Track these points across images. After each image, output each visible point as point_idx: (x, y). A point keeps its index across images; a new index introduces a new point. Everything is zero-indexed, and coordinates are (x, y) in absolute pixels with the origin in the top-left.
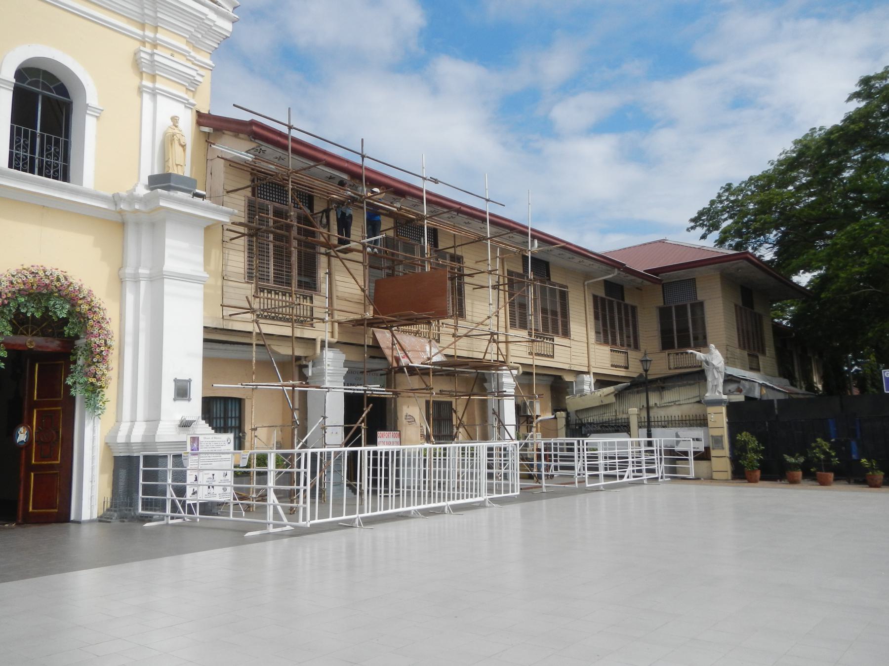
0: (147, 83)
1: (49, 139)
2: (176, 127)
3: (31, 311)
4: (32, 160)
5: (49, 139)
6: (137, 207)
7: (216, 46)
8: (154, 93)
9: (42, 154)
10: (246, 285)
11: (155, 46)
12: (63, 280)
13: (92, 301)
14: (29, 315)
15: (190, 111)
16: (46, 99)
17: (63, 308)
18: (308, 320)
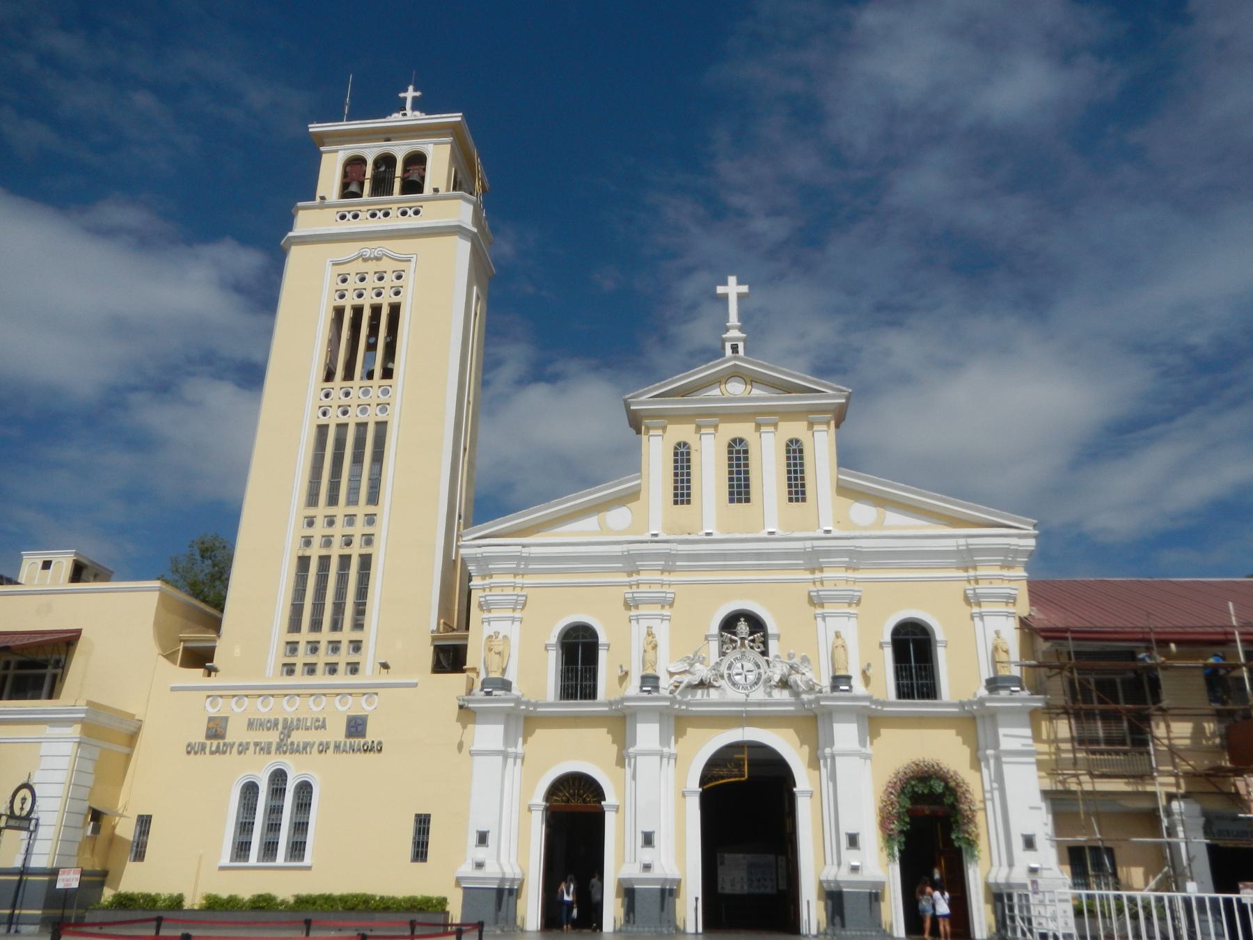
0: (976, 610)
1: (920, 668)
2: (999, 638)
3: (920, 789)
4: (912, 684)
5: (920, 668)
6: (975, 707)
7: (1026, 560)
8: (981, 616)
9: (917, 680)
11: (977, 581)
12: (936, 767)
13: (957, 778)
14: (920, 792)
15: (1012, 619)
16: (916, 643)
17: (940, 785)
18: (1145, 775)
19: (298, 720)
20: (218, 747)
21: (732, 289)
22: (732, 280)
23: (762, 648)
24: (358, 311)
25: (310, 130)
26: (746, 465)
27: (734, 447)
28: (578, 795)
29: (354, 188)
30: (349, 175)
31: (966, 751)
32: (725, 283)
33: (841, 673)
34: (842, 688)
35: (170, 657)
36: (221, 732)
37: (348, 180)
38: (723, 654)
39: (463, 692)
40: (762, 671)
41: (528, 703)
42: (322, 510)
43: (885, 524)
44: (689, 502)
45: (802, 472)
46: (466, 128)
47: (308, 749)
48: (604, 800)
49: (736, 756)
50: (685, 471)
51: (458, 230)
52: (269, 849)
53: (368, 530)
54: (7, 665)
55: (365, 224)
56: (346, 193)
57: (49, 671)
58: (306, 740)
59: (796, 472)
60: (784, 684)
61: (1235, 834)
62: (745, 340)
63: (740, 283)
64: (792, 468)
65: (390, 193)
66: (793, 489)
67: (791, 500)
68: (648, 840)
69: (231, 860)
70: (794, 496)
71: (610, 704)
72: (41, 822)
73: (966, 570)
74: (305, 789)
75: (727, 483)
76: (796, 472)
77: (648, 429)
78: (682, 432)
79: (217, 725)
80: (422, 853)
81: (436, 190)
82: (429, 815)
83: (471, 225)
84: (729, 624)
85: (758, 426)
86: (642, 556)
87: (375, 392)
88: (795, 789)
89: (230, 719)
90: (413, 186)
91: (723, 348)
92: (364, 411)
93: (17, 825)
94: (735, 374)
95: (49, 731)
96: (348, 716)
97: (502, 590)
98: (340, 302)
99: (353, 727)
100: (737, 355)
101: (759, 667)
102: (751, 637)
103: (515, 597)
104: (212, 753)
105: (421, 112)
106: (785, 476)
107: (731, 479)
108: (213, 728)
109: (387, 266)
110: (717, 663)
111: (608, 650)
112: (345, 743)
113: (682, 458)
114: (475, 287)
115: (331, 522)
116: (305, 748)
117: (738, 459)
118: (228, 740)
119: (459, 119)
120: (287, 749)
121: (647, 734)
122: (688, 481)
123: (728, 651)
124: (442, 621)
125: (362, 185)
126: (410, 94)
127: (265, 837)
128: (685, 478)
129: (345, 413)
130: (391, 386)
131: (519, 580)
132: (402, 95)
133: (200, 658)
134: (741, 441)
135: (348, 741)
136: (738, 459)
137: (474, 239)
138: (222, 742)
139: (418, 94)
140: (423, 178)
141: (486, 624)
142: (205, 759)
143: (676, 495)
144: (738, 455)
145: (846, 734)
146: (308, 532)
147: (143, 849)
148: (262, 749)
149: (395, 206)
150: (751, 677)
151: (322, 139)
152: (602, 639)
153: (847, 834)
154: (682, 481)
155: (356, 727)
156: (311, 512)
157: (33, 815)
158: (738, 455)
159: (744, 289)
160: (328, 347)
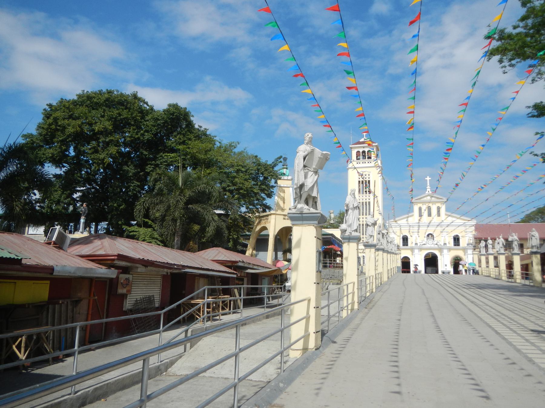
3: (456, 259)
21: (428, 178)
22: (428, 177)
29: (358, 158)
31: (463, 253)
56: (357, 159)
60: (437, 244)
63: (429, 177)
65: (365, 159)
73: (465, 227)
77: (414, 205)
84: (428, 235)
85: (433, 204)
86: (415, 225)
87: (368, 196)
90: (370, 158)
92: (366, 200)
94: (428, 195)
98: (359, 180)
113: (420, 209)
115: (363, 218)
121: (416, 251)
145: (445, 251)
150: (432, 243)
151: (351, 148)
152: (408, 238)
158: (429, 209)
159: (430, 179)
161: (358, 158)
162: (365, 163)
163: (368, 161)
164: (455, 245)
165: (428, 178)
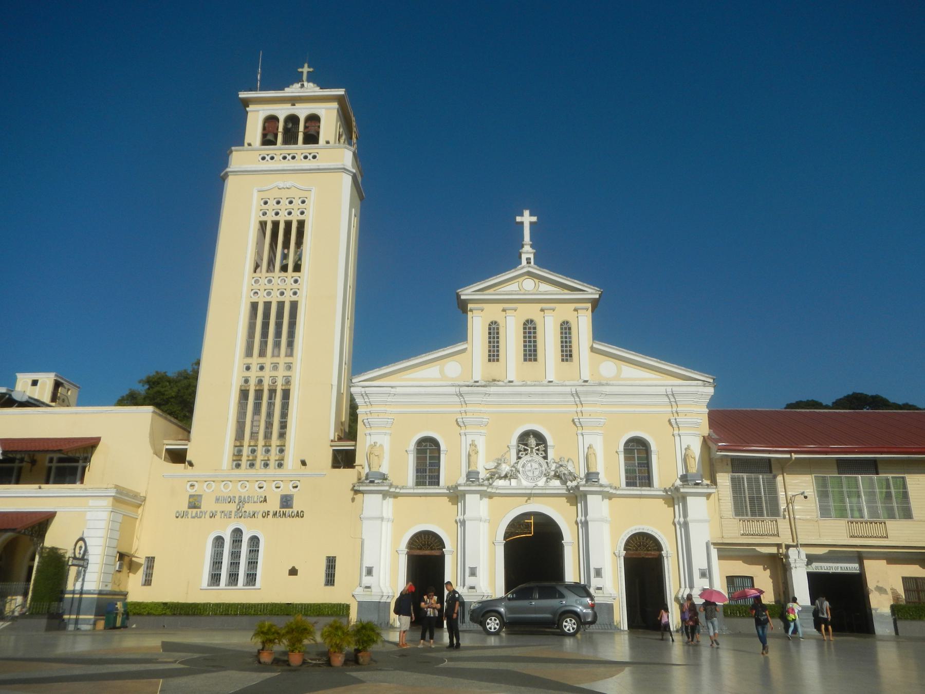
0: (676, 432)
10: (733, 520)
19: (249, 497)
20: (197, 513)
21: (527, 219)
22: (527, 213)
23: (544, 455)
24: (276, 224)
25: (240, 96)
26: (535, 337)
27: (526, 325)
28: (427, 545)
30: (267, 128)
32: (522, 215)
33: (592, 470)
34: (593, 480)
35: (157, 454)
36: (198, 504)
37: (266, 132)
38: (519, 458)
39: (355, 480)
40: (543, 468)
41: (396, 487)
42: (255, 361)
43: (622, 376)
44: (498, 360)
45: (570, 342)
46: (347, 100)
47: (256, 515)
48: (445, 548)
49: (526, 521)
50: (496, 340)
51: (345, 170)
52: (233, 578)
53: (287, 373)
54: (51, 460)
55: (278, 164)
57: (80, 464)
58: (255, 510)
59: (566, 342)
61: (826, 568)
62: (535, 254)
63: (531, 215)
64: (564, 340)
65: (296, 143)
66: (565, 353)
67: (563, 360)
68: (473, 573)
69: (208, 586)
70: (565, 358)
71: (448, 488)
72: (89, 562)
74: (255, 540)
75: (522, 348)
76: (566, 342)
77: (471, 310)
78: (493, 312)
79: (195, 500)
80: (331, 580)
81: (328, 142)
82: (335, 557)
83: (351, 166)
84: (524, 437)
88: (563, 542)
89: (203, 496)
90: (312, 138)
91: (520, 258)
92: (282, 294)
93: (77, 564)
95: (92, 502)
96: (281, 495)
97: (378, 416)
98: (264, 218)
99: (285, 502)
100: (530, 265)
101: (541, 466)
102: (537, 448)
103: (387, 420)
104: (193, 517)
105: (314, 83)
106: (559, 344)
107: (525, 346)
108: (192, 502)
109: (297, 195)
110: (516, 463)
111: (446, 454)
112: (280, 511)
113: (494, 332)
114: (353, 210)
115: (262, 368)
116: (254, 515)
117: (530, 333)
118: (203, 508)
119: (343, 93)
120: (242, 515)
122: (498, 347)
123: (522, 456)
124: (336, 434)
125: (276, 136)
126: (306, 69)
127: (229, 570)
128: (496, 344)
129: (269, 294)
130: (300, 277)
131: (389, 409)
132: (300, 70)
133: (178, 457)
134: (532, 321)
135: (282, 510)
136: (530, 333)
137: (354, 178)
138: (198, 510)
139: (311, 70)
140: (318, 133)
141: (368, 437)
142: (188, 521)
143: (490, 356)
144: (530, 330)
146: (247, 374)
147: (150, 578)
148: (225, 515)
149: (299, 152)
150: (537, 473)
151: (246, 103)
153: (594, 568)
154: (494, 347)
155: (286, 501)
156: (249, 360)
157: (85, 557)
158: (530, 330)
159: (534, 219)
160: (256, 249)
161: (270, 137)
162: (293, 158)
163: (306, 152)
164: (630, 483)
165: (527, 219)
